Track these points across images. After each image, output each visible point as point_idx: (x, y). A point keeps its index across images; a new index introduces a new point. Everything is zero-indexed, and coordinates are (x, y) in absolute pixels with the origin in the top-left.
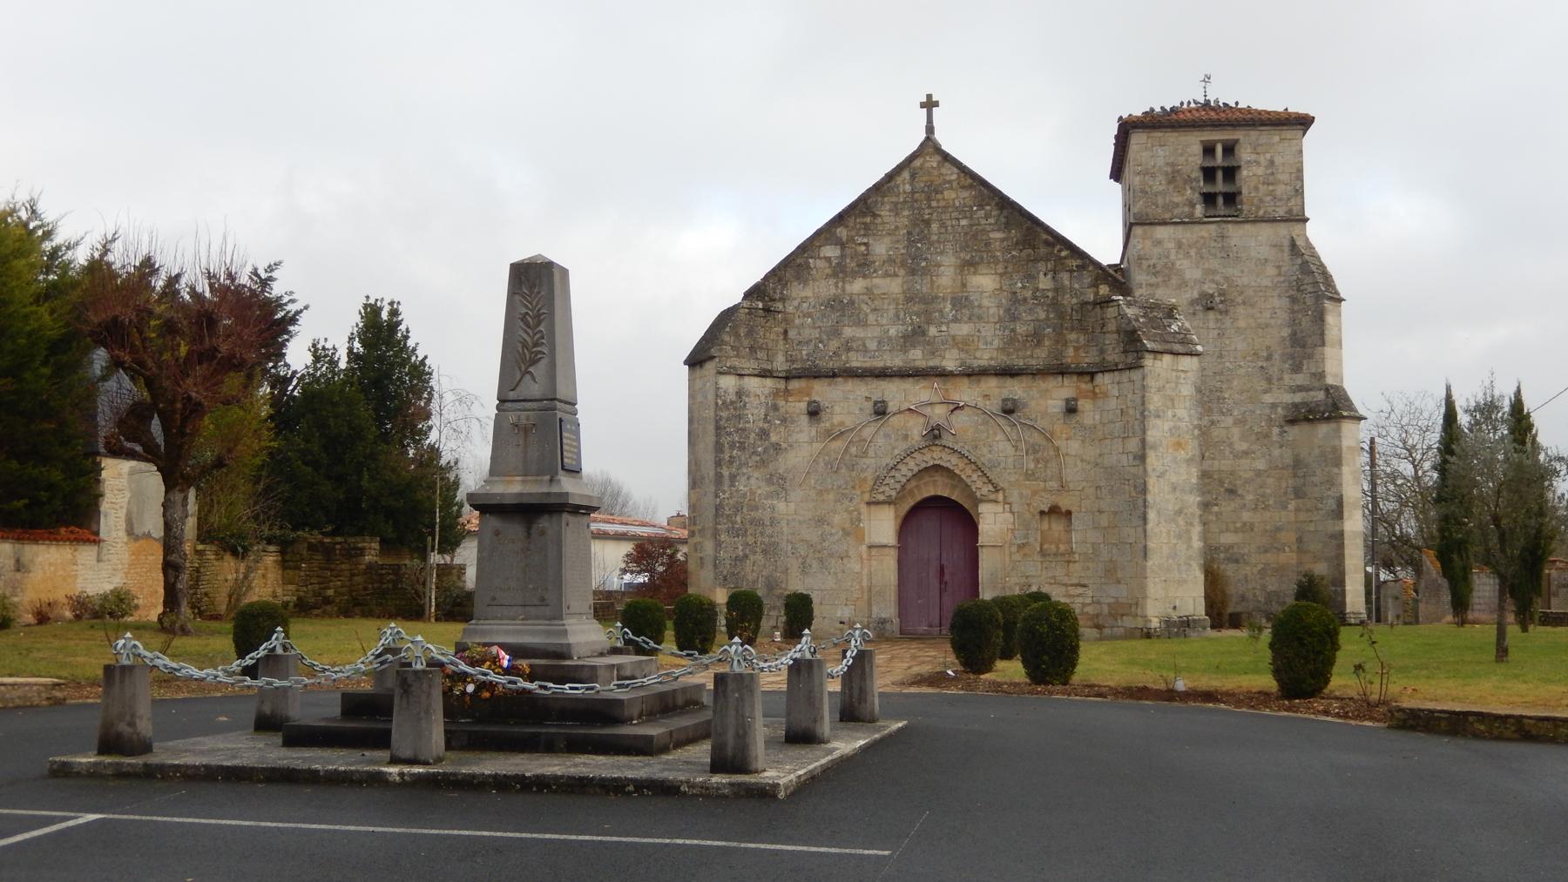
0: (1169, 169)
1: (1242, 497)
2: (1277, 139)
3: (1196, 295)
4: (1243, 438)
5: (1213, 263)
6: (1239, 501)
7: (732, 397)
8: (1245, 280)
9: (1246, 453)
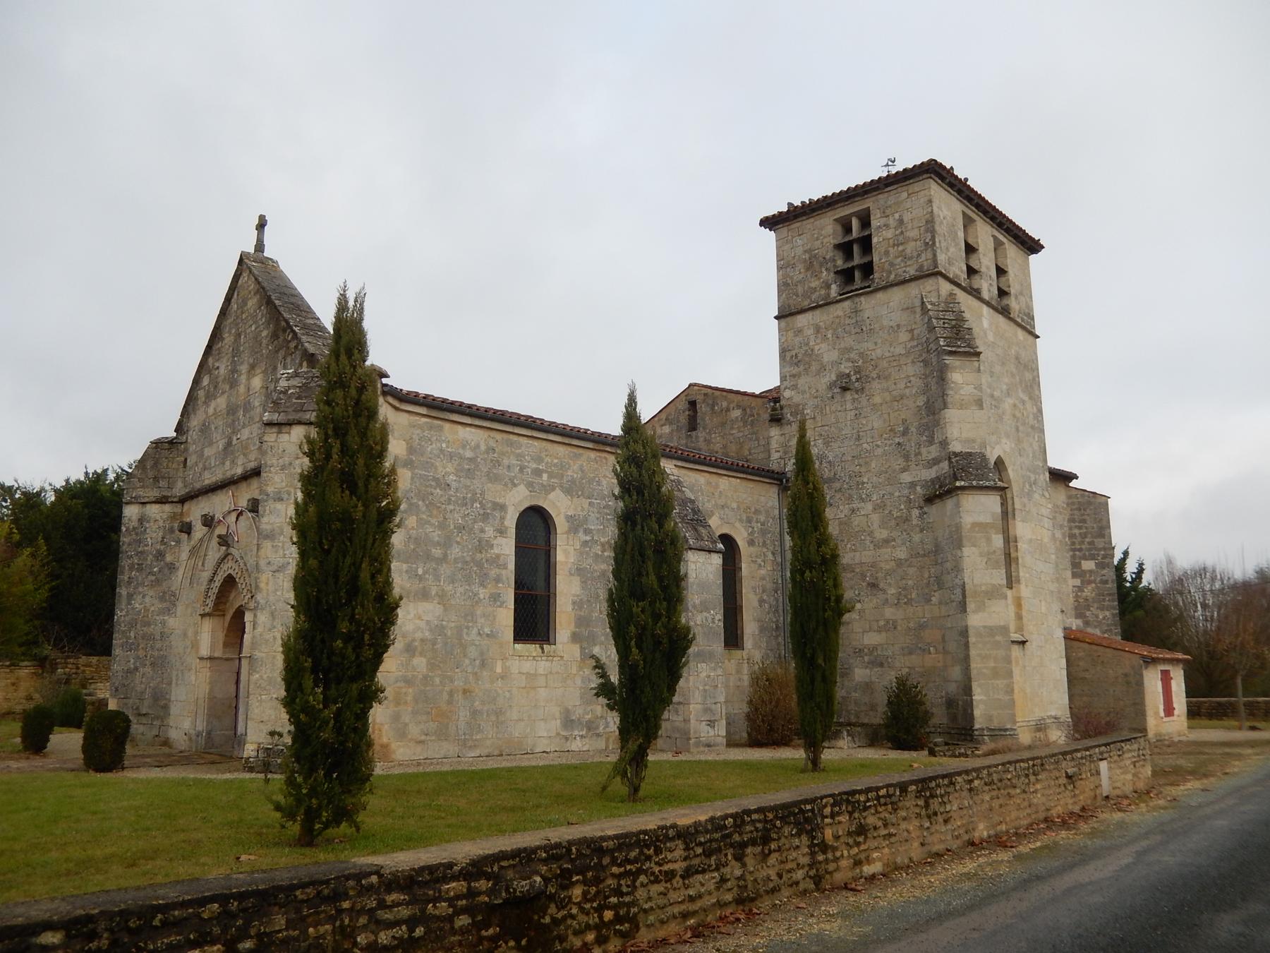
0: (807, 256)
1: (884, 591)
2: (905, 195)
3: (834, 377)
4: (883, 525)
5: (849, 341)
6: (881, 596)
7: (135, 523)
8: (879, 352)
9: (886, 541)
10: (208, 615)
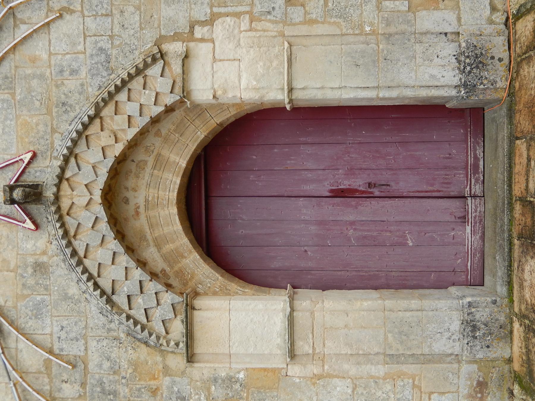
10: (190, 308)
